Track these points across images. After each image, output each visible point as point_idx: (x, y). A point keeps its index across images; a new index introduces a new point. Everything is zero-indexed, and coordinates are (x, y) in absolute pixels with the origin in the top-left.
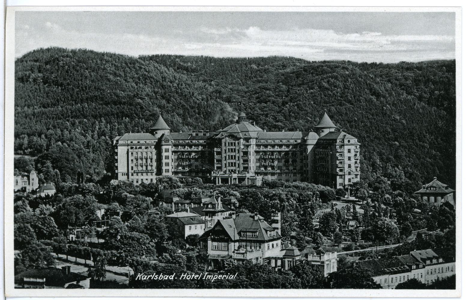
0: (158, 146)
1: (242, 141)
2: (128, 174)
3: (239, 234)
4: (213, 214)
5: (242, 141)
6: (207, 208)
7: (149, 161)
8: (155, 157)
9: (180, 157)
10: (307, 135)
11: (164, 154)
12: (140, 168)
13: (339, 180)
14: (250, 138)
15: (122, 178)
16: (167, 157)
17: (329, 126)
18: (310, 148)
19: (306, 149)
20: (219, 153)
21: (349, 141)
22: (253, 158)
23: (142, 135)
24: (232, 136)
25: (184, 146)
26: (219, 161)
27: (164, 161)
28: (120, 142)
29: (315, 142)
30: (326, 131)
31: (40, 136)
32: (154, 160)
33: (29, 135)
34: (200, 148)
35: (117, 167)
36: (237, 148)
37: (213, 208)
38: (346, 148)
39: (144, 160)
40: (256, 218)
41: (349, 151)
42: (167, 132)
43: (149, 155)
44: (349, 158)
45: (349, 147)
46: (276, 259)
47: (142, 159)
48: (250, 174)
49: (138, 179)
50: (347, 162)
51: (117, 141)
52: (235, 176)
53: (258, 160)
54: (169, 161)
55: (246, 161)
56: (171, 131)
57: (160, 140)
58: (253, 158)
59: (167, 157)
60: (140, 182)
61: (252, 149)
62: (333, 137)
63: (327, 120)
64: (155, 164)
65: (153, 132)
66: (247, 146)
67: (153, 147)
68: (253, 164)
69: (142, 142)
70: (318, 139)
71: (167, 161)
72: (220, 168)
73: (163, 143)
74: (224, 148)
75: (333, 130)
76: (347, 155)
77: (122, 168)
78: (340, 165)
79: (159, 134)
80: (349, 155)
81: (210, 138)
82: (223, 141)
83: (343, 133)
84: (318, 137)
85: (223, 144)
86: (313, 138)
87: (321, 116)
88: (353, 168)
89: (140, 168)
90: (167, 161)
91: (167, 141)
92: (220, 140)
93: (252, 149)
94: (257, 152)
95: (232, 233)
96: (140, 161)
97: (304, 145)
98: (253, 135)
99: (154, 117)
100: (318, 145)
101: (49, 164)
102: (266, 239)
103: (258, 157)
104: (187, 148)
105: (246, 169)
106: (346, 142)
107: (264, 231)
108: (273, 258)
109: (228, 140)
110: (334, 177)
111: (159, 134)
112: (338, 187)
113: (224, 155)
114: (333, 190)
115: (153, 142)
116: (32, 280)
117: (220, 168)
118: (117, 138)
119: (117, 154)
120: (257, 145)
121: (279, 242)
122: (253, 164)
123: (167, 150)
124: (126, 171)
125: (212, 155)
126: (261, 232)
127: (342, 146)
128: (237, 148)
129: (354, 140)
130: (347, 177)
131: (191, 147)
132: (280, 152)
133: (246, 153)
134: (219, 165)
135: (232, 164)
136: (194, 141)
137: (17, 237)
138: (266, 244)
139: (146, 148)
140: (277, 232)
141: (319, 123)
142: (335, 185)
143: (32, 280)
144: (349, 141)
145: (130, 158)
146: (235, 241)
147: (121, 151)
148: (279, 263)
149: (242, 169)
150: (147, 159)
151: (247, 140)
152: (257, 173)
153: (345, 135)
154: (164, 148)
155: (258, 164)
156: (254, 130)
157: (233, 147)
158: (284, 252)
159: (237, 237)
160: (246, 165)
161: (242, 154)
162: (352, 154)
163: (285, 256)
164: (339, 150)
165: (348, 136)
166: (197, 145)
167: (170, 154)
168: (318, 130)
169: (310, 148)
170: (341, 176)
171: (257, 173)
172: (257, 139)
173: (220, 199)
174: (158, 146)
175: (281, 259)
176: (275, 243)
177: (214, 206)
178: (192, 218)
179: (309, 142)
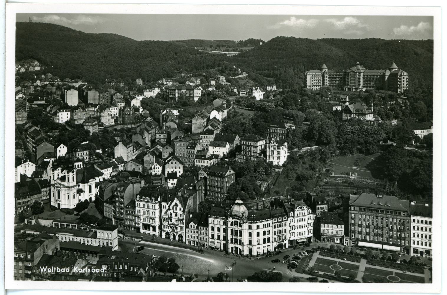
0: (323, 76)
1: (357, 73)
2: (311, 86)
3: (356, 111)
4: (345, 102)
5: (357, 73)
6: (343, 100)
7: (319, 81)
8: (322, 80)
9: (332, 79)
10: (385, 71)
11: (325, 78)
12: (316, 84)
13: (399, 90)
14: (361, 72)
15: (308, 87)
16: (327, 80)
17: (395, 67)
18: (387, 77)
19: (385, 78)
20: (348, 78)
21: (404, 74)
22: (362, 80)
23: (317, 71)
24: (353, 72)
25: (333, 75)
26: (348, 81)
27: (325, 81)
28: (308, 74)
29: (389, 74)
30: (394, 70)
31: (277, 70)
32: (321, 81)
33: (273, 70)
35: (307, 83)
36: (355, 76)
37: (345, 100)
38: (402, 77)
39: (317, 81)
40: (363, 105)
41: (404, 78)
42: (326, 70)
43: (320, 79)
44: (404, 81)
45: (404, 76)
46: (371, 121)
47: (316, 80)
48: (361, 87)
49: (315, 88)
50: (402, 83)
51: (307, 73)
52: (354, 88)
53: (364, 81)
54: (328, 81)
55: (359, 82)
56: (328, 70)
57: (324, 73)
58: (362, 80)
59: (327, 80)
60: (315, 89)
61: (361, 77)
62: (397, 72)
63: (395, 65)
64: (322, 82)
66: (360, 76)
67: (321, 76)
68: (362, 83)
69: (316, 74)
70: (390, 73)
71: (326, 81)
72: (348, 84)
73: (325, 74)
74: (350, 76)
75: (397, 69)
76: (403, 80)
77: (309, 84)
78: (399, 84)
80: (404, 80)
81: (345, 72)
82: (350, 73)
83: (401, 71)
84: (390, 72)
85: (350, 75)
86: (388, 73)
87: (392, 63)
88: (405, 85)
89: (316, 84)
90: (326, 81)
91: (327, 73)
92: (348, 73)
93: (361, 77)
94: (364, 78)
95: (353, 110)
96: (316, 81)
97: (384, 76)
98: (362, 71)
99: (321, 64)
100: (389, 76)
101: (281, 81)
102: (367, 113)
103: (364, 80)
105: (359, 85)
106: (402, 74)
107: (366, 110)
108: (369, 121)
110: (397, 88)
111: (324, 70)
112: (398, 93)
113: (350, 79)
114: (396, 94)
116: (273, 126)
117: (348, 84)
118: (307, 72)
119: (307, 78)
120: (364, 75)
121: (372, 114)
122: (362, 83)
123: (327, 77)
124: (310, 85)
125: (344, 78)
126: (365, 110)
127: (401, 76)
128: (355, 76)
129: (406, 74)
130: (403, 89)
131: (336, 75)
132: (373, 78)
133: (359, 79)
134: (348, 83)
135: (353, 83)
136: (337, 74)
137: (429, 171)
138: (367, 115)
139: (318, 76)
140: (372, 110)
141: (391, 66)
142: (397, 92)
143: (273, 126)
144: (404, 74)
145: (312, 80)
146: (354, 114)
147: (309, 77)
148: (372, 123)
149: (357, 85)
150: (318, 80)
151: (360, 73)
152: (364, 87)
153: (402, 72)
154: (325, 76)
155: (364, 83)
156: (362, 69)
157: (354, 76)
158: (374, 119)
159: (355, 112)
160: (359, 83)
161: (357, 79)
162: (405, 80)
163: (375, 120)
164: (399, 78)
165: (404, 72)
166: (339, 75)
167: (328, 78)
168: (390, 69)
169: (387, 77)
170: (400, 88)
171: (364, 87)
172: (363, 73)
173: (348, 97)
174: (323, 76)
175: (373, 121)
176: (370, 115)
177: (345, 99)
178: (336, 104)
179: (386, 74)
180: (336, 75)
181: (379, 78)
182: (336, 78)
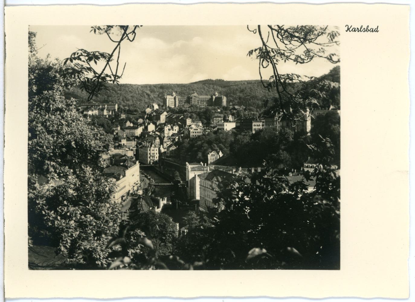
0: (175, 99)
9: (180, 101)
18: (214, 99)
19: (213, 100)
20: (191, 101)
24: (195, 96)
34: (185, 100)
65: (172, 95)
79: (174, 96)
86: (214, 97)
100: (215, 99)
104: (181, 100)
109: (194, 97)
115: (173, 97)
131: (182, 99)
166: (184, 99)
168: (215, 95)
169: (214, 99)
174: (175, 99)
180: (182, 99)
181: (209, 100)
182: (182, 101)
